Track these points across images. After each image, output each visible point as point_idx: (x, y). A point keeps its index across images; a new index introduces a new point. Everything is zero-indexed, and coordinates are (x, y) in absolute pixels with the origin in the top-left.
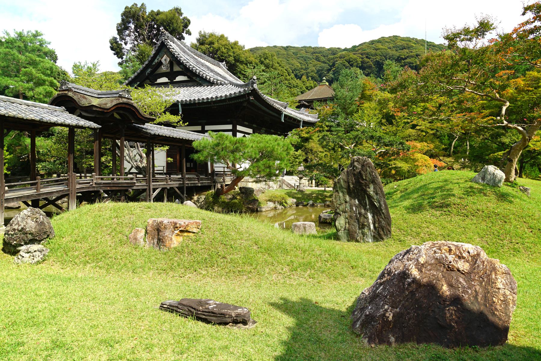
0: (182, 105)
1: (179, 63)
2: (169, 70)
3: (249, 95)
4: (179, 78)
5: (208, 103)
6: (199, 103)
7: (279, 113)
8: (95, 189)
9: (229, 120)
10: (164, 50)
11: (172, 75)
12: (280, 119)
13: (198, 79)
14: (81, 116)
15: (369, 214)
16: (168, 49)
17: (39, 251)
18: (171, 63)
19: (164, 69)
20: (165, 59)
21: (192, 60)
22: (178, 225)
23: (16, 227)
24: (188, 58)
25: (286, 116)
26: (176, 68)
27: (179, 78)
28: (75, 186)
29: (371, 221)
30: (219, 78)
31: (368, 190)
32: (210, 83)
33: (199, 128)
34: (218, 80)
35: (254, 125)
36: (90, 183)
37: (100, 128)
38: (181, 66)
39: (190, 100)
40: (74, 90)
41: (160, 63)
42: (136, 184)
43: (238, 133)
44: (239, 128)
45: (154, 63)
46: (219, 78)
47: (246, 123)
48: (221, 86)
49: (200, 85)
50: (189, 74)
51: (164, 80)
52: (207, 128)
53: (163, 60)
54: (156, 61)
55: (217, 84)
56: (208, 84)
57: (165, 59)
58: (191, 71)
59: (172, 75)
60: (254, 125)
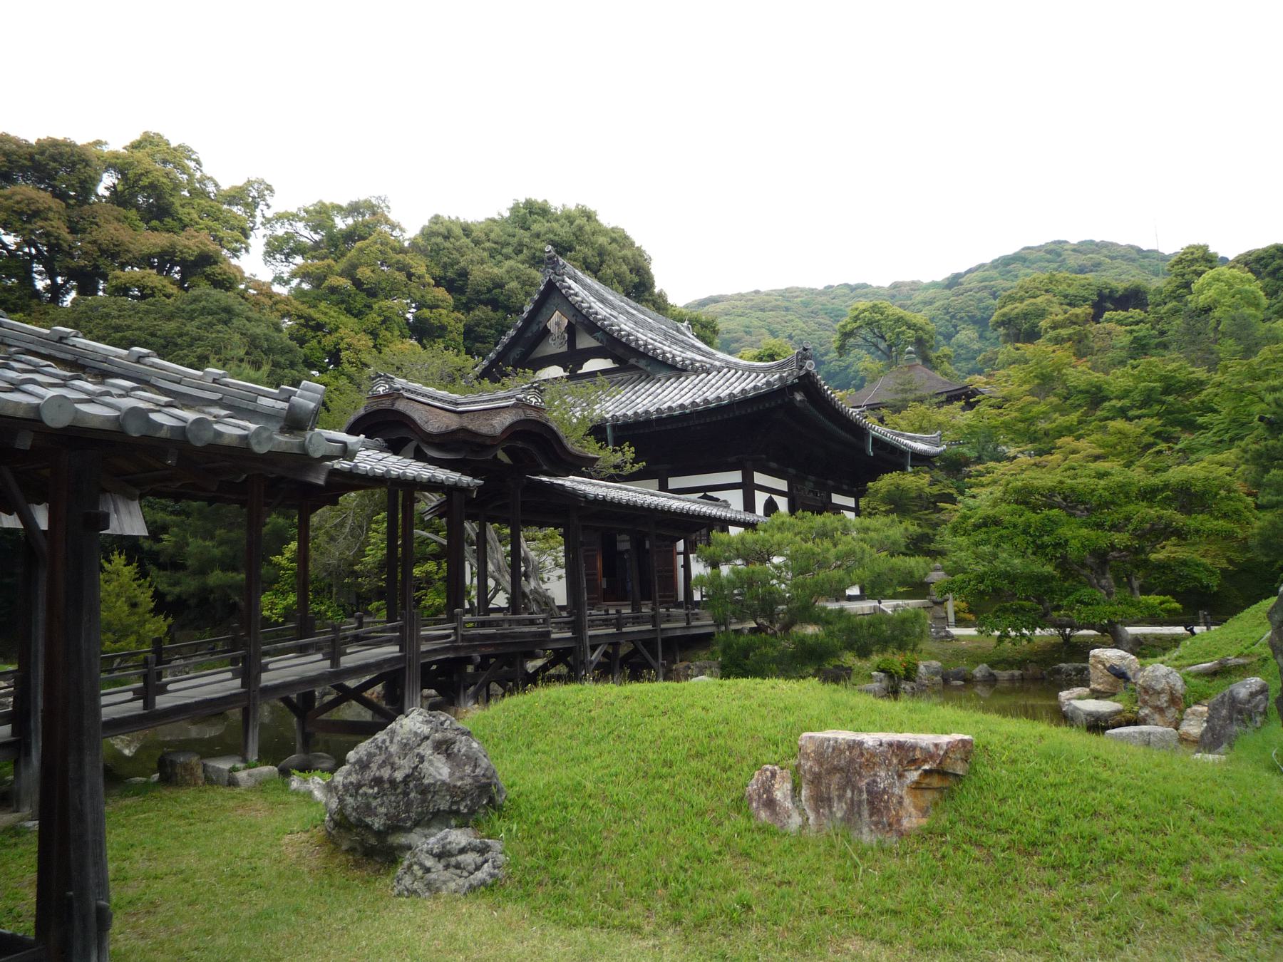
2: (564, 349)
3: (792, 388)
5: (683, 417)
6: (659, 420)
7: (859, 431)
8: (462, 654)
9: (732, 459)
10: (556, 300)
11: (573, 359)
12: (864, 451)
13: (642, 364)
14: (419, 456)
16: (566, 298)
17: (474, 849)
18: (571, 329)
19: (555, 346)
20: (557, 321)
21: (622, 318)
22: (918, 755)
23: (386, 773)
24: (615, 313)
25: (875, 440)
26: (585, 342)
27: (592, 365)
28: (418, 647)
30: (699, 358)
32: (676, 370)
34: (693, 361)
35: (792, 471)
36: (448, 636)
37: (479, 487)
38: (598, 334)
39: (636, 413)
40: (406, 394)
41: (546, 332)
42: (553, 636)
44: (759, 478)
46: (699, 358)
47: (773, 465)
48: (704, 375)
49: (649, 377)
50: (619, 351)
51: (555, 371)
52: (674, 483)
53: (551, 325)
54: (535, 328)
55: (696, 372)
56: (669, 373)
57: (557, 321)
58: (626, 346)
59: (573, 359)
60: (790, 470)
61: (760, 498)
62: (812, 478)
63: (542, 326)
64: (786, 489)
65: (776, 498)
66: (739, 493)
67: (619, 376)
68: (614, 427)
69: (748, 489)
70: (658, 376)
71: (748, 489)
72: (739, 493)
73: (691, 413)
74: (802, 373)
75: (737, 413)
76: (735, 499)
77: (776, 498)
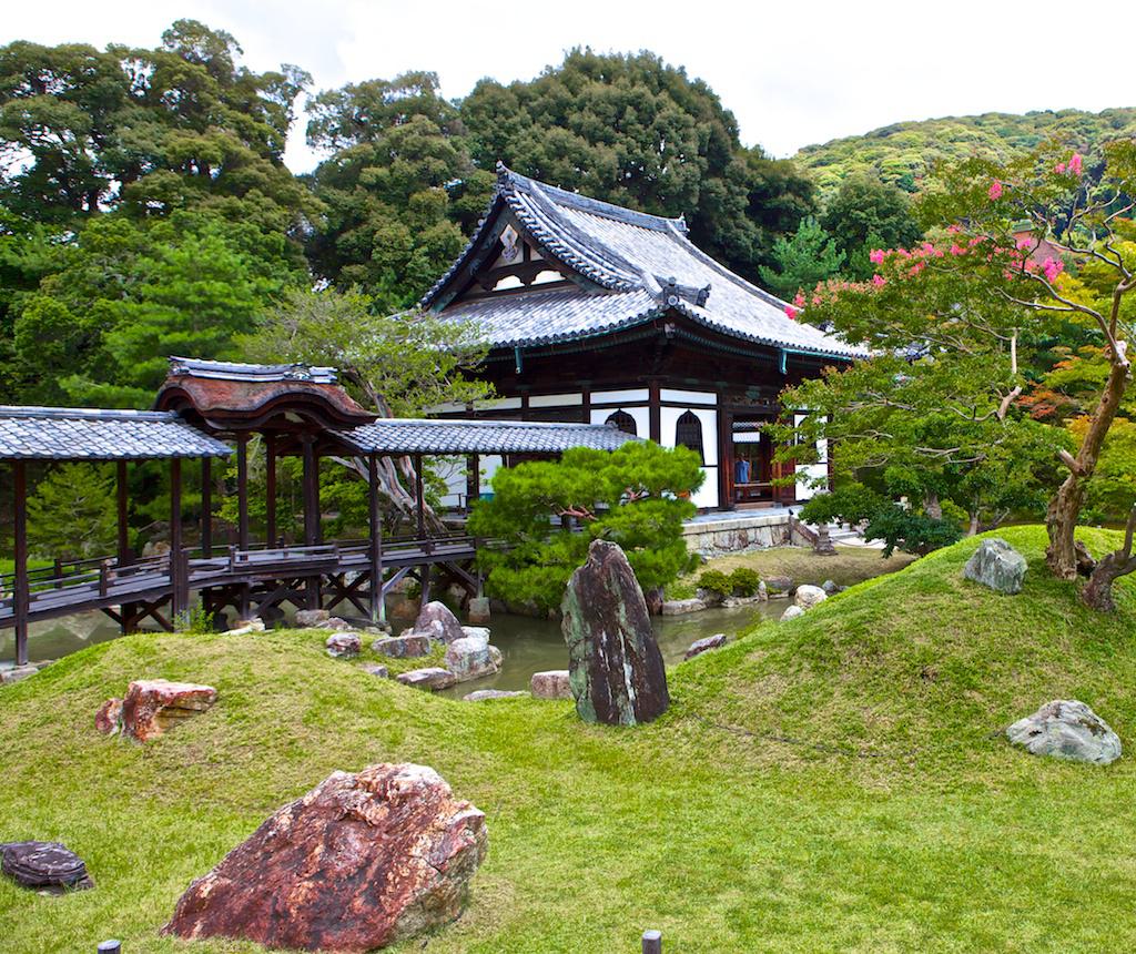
0: (521, 349)
1: (539, 245)
3: (661, 321)
4: (545, 277)
11: (527, 271)
13: (577, 279)
15: (625, 665)
27: (545, 277)
29: (628, 681)
31: (617, 615)
32: (605, 289)
35: (721, 384)
41: (500, 246)
43: (663, 409)
44: (666, 395)
45: (486, 247)
49: (582, 295)
51: (512, 282)
52: (596, 398)
53: (504, 238)
54: (490, 241)
55: (618, 291)
56: (598, 290)
57: (509, 235)
59: (527, 271)
60: (718, 383)
61: (670, 418)
62: (757, 388)
63: (496, 238)
64: (714, 402)
65: (695, 412)
66: (646, 410)
67: (564, 290)
68: (521, 349)
69: (655, 405)
70: (590, 292)
71: (655, 405)
72: (646, 410)
73: (581, 340)
74: (667, 307)
75: (617, 342)
76: (641, 416)
77: (695, 412)
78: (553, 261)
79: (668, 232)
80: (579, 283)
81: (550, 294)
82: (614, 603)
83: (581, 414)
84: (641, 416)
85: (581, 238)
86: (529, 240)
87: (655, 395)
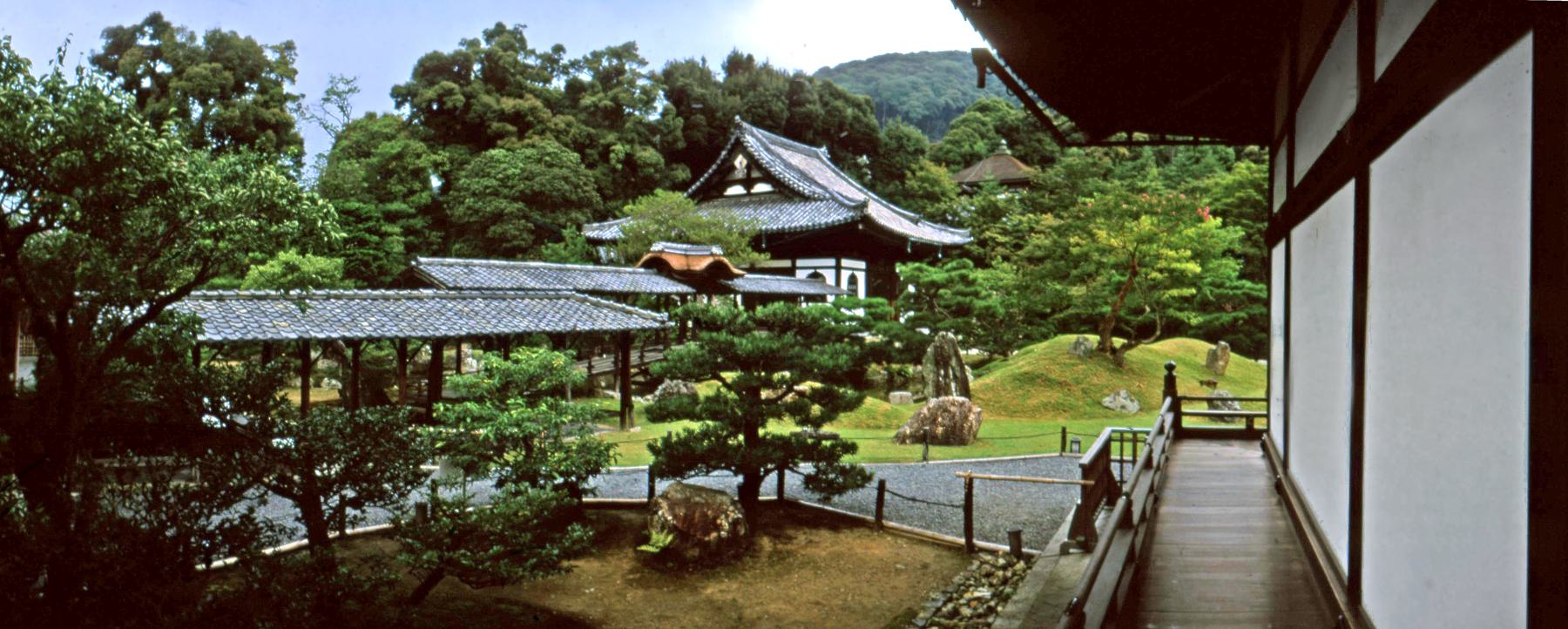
11: (748, 183)
18: (748, 167)
20: (740, 161)
26: (755, 174)
33: (786, 263)
41: (733, 168)
44: (845, 262)
52: (800, 263)
53: (737, 163)
55: (815, 200)
57: (740, 161)
59: (748, 183)
61: (845, 275)
66: (833, 272)
69: (838, 268)
71: (838, 268)
76: (830, 276)
78: (768, 177)
79: (818, 157)
80: (785, 193)
81: (761, 200)
82: (950, 358)
83: (790, 272)
84: (830, 276)
85: (788, 166)
86: (753, 163)
87: (838, 263)
